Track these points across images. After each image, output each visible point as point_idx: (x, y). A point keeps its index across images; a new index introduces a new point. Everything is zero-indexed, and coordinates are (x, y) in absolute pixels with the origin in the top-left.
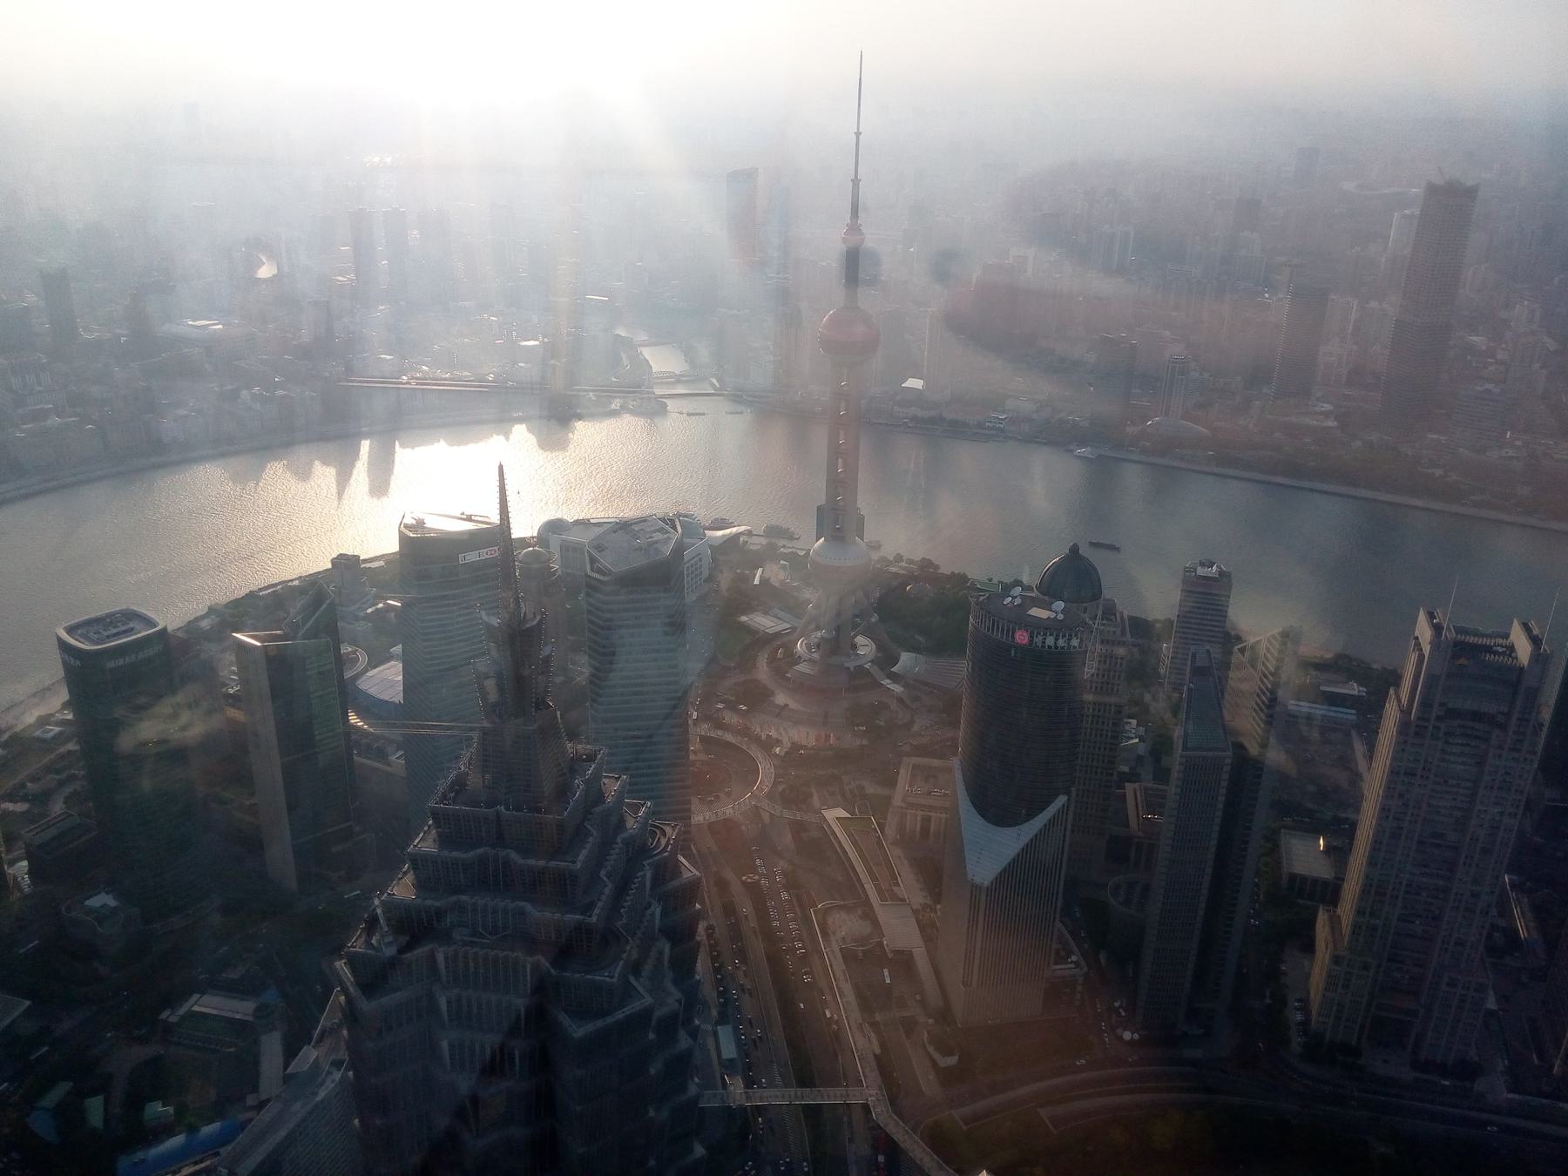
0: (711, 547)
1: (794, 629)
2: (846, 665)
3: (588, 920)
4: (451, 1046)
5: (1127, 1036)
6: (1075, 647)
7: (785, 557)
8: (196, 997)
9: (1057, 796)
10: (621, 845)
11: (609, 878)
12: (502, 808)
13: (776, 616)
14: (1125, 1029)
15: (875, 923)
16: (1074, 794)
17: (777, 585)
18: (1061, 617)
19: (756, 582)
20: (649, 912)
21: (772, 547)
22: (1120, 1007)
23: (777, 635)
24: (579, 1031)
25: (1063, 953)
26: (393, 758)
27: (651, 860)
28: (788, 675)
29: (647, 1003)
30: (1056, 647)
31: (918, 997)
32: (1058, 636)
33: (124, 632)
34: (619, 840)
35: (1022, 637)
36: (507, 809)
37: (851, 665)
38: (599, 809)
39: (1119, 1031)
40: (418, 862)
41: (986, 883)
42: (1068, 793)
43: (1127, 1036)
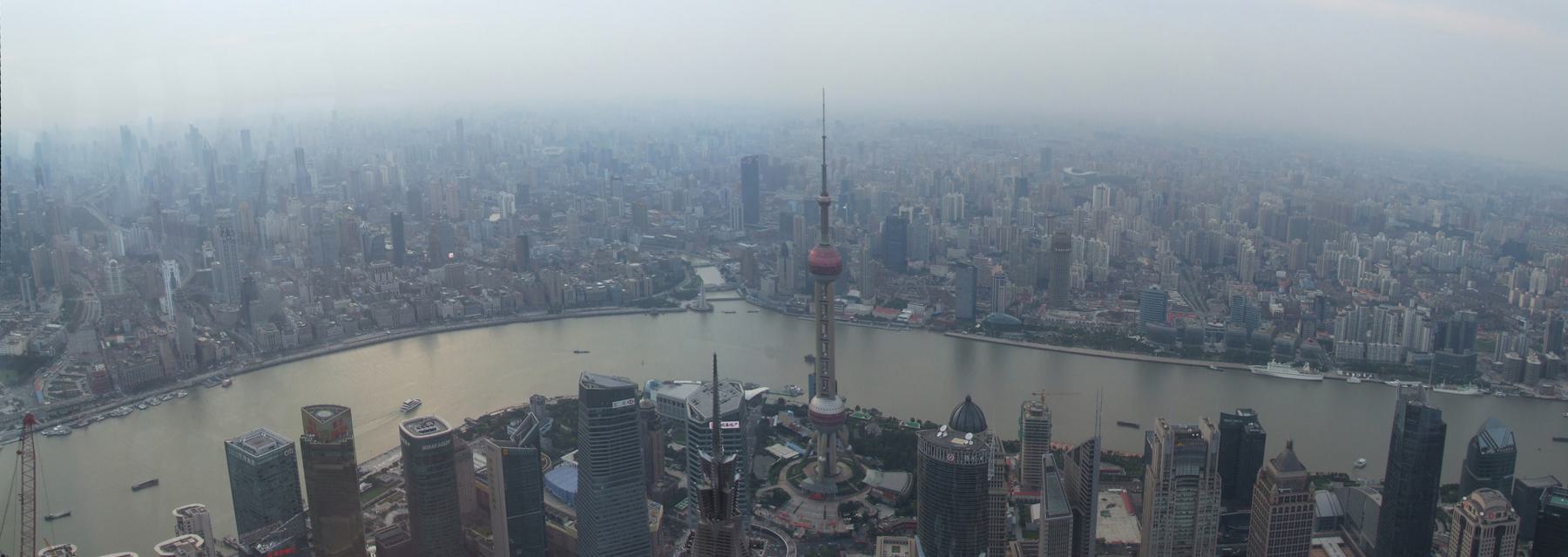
1: (801, 455)
23: (791, 459)
28: (800, 486)
33: (432, 430)
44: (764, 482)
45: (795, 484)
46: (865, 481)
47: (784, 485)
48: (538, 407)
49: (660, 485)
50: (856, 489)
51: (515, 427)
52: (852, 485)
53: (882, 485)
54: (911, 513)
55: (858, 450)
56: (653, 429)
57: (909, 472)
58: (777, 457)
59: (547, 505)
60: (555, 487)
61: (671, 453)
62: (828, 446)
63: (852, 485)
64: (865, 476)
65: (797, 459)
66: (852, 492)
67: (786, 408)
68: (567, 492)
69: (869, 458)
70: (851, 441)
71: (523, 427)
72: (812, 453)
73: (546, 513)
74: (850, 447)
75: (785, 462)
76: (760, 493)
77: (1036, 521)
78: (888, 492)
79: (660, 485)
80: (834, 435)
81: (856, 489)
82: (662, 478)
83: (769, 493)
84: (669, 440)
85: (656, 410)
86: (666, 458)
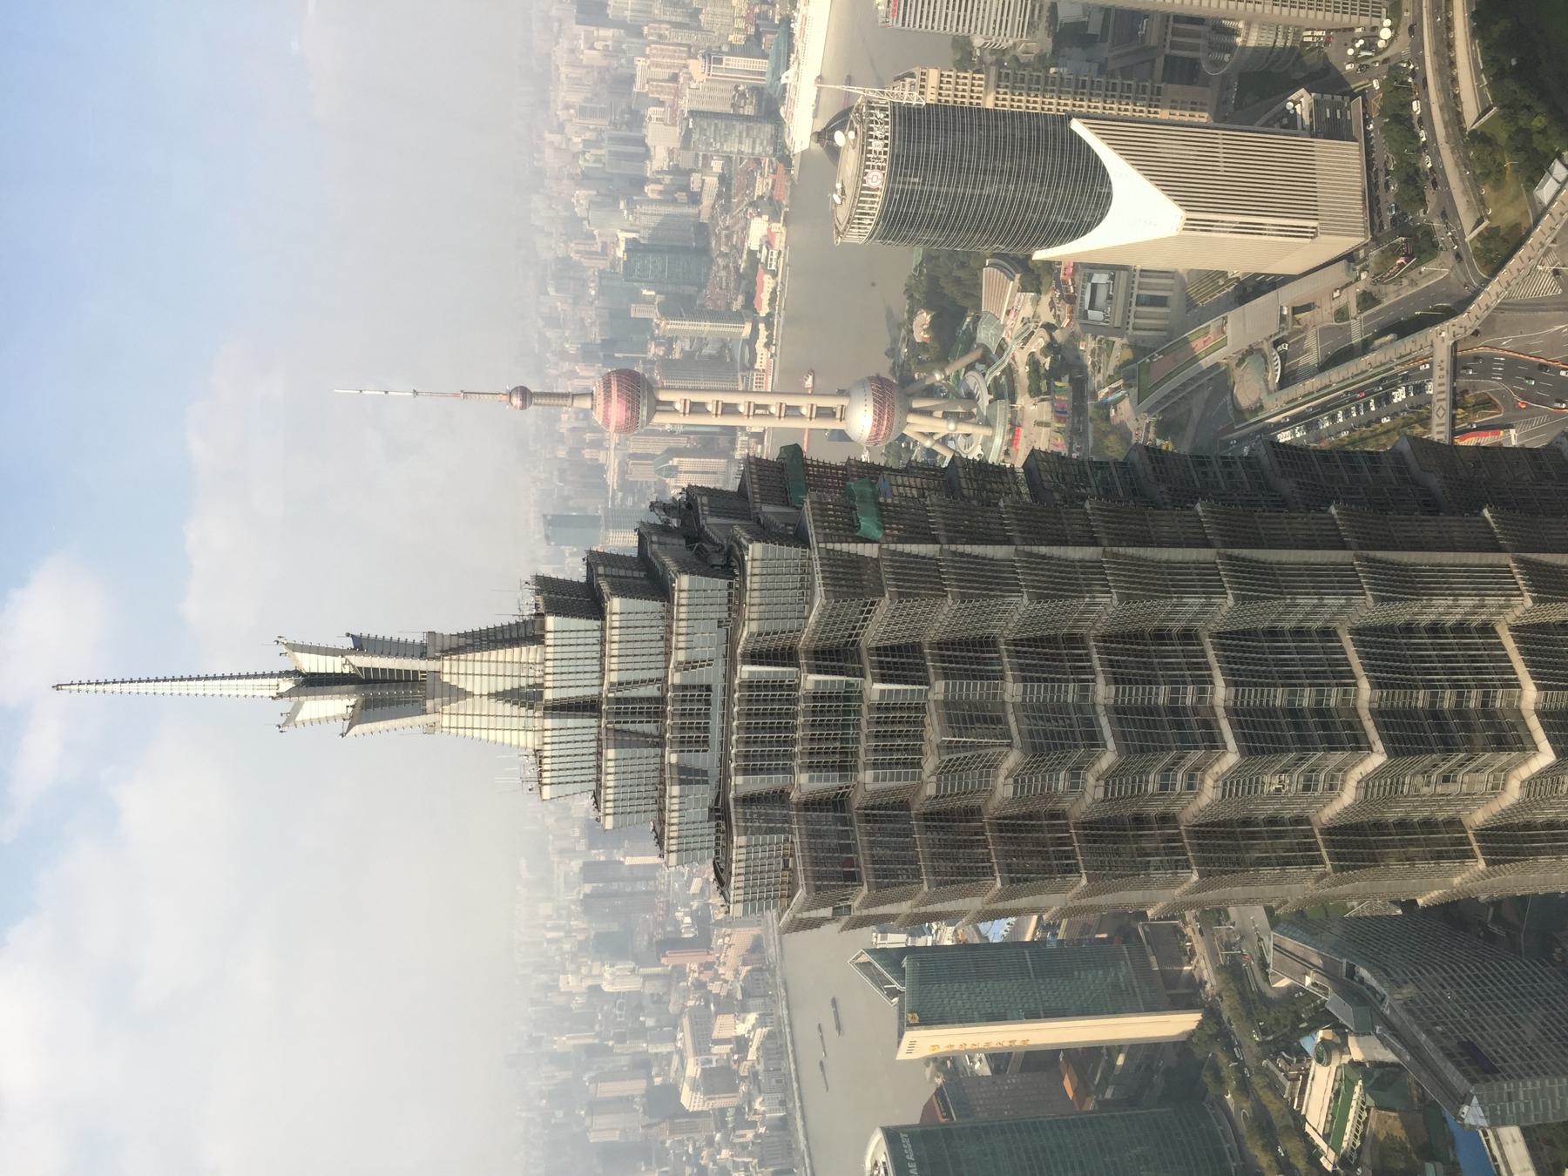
2: (987, 403)
5: (1385, 34)
6: (887, 116)
8: (1308, 1129)
9: (1071, 131)
14: (1378, 38)
15: (1250, 351)
22: (1353, 47)
25: (1285, 121)
30: (886, 138)
31: (1336, 294)
32: (871, 136)
35: (876, 179)
37: (985, 399)
39: (1381, 44)
42: (1069, 117)
43: (1385, 34)
64: (986, 350)
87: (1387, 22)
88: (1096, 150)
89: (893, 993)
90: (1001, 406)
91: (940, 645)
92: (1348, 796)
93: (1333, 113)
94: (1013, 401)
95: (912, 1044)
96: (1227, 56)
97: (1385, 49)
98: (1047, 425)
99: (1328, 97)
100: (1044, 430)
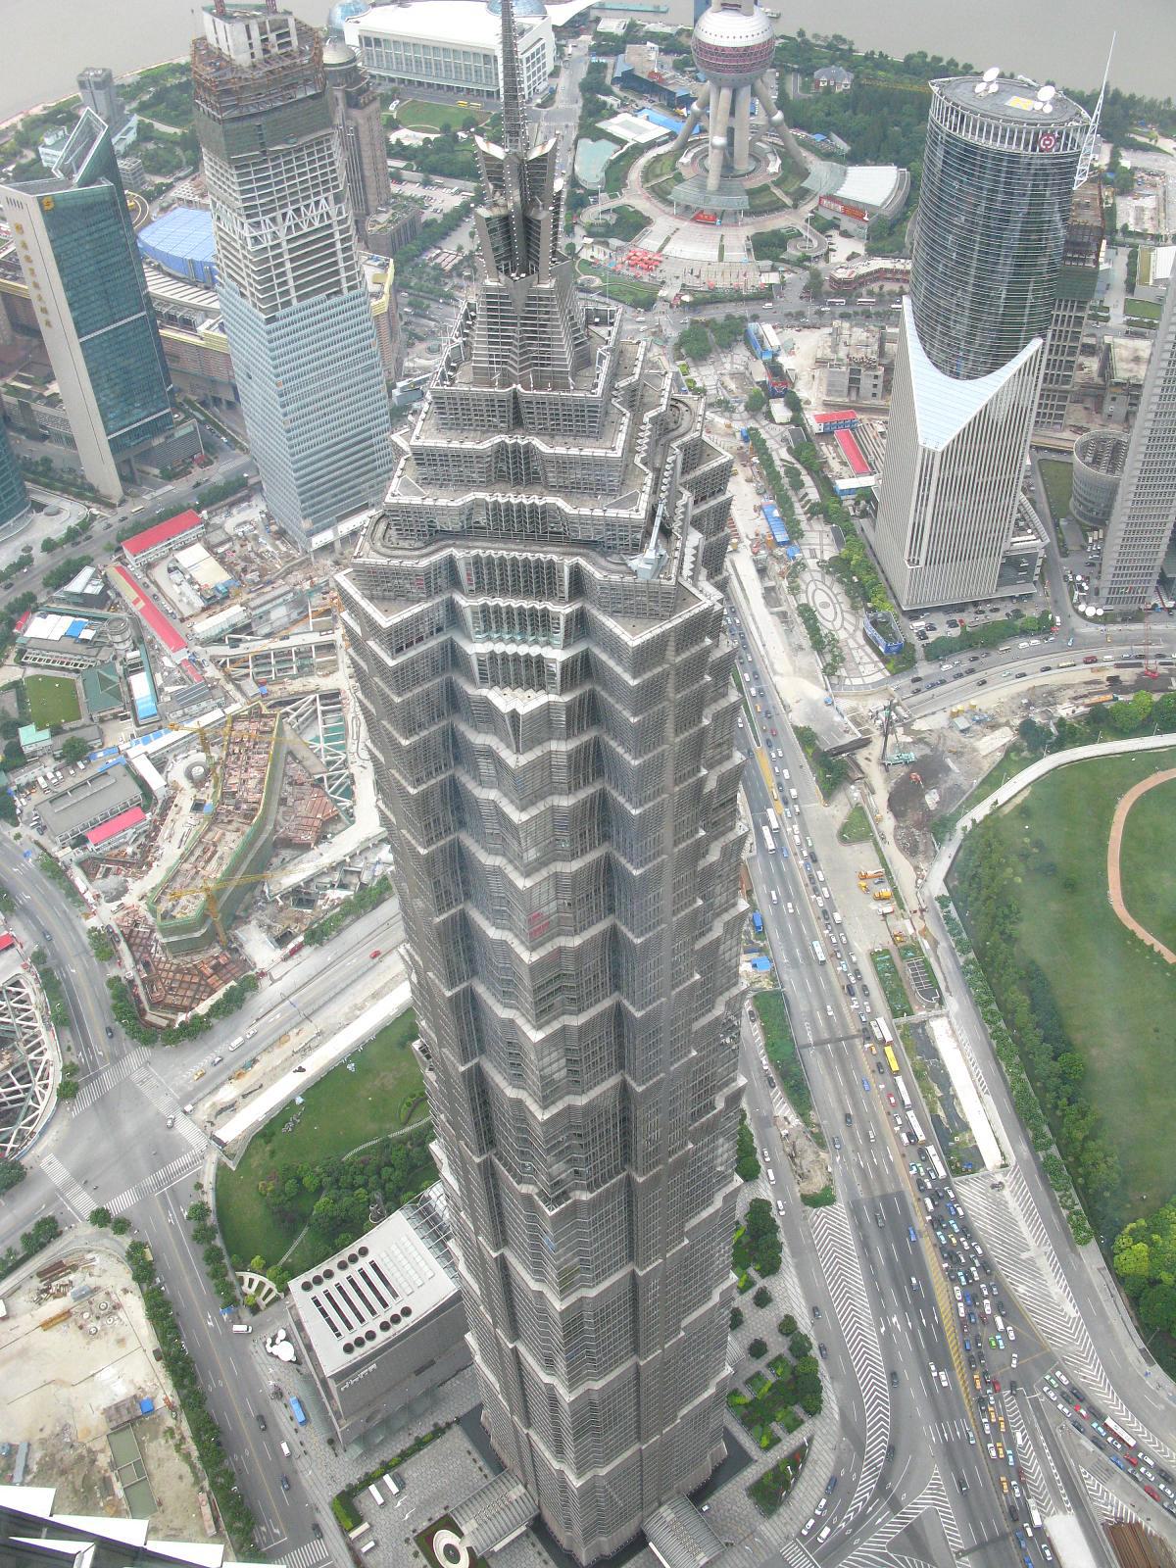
0: (554, 27)
1: (672, 136)
3: (635, 516)
4: (481, 663)
5: (1090, 611)
7: (653, 37)
10: (649, 426)
11: (645, 464)
12: (519, 387)
13: (648, 118)
16: (1050, 335)
17: (645, 77)
18: (1048, 109)
19: (618, 74)
20: (680, 503)
21: (631, 28)
24: (633, 636)
25: (1022, 524)
26: (201, 329)
27: (679, 442)
29: (706, 606)
34: (646, 419)
36: (527, 388)
38: (623, 383)
39: (1082, 608)
40: (422, 457)
41: (940, 450)
42: (1044, 337)
43: (1090, 611)
44: (595, 193)
45: (661, 194)
46: (806, 184)
47: (635, 197)
48: (100, 95)
49: (383, 218)
50: (788, 201)
51: (56, 146)
52: (778, 192)
53: (840, 193)
54: (897, 252)
55: (795, 120)
56: (356, 106)
57: (899, 164)
58: (621, 142)
59: (157, 297)
60: (169, 259)
61: (401, 151)
62: (732, 113)
63: (778, 192)
64: (805, 174)
65: (665, 142)
66: (777, 207)
67: (642, 41)
68: (192, 261)
69: (818, 138)
70: (783, 103)
71: (77, 142)
72: (697, 130)
73: (158, 314)
74: (779, 116)
75: (639, 150)
76: (590, 214)
77: (1156, 281)
78: (854, 210)
79: (383, 218)
80: (745, 92)
81: (788, 201)
82: (387, 204)
83: (607, 217)
84: (393, 125)
85: (360, 64)
86: (390, 163)
87: (1100, 612)
88: (1009, 364)
89: (68, 173)
90: (742, 202)
91: (592, 696)
92: (493, 933)
93: (1024, 569)
94: (747, 214)
95: (19, 205)
96: (1089, 459)
97: (1077, 611)
98: (721, 258)
99: (1039, 562)
100: (716, 253)
